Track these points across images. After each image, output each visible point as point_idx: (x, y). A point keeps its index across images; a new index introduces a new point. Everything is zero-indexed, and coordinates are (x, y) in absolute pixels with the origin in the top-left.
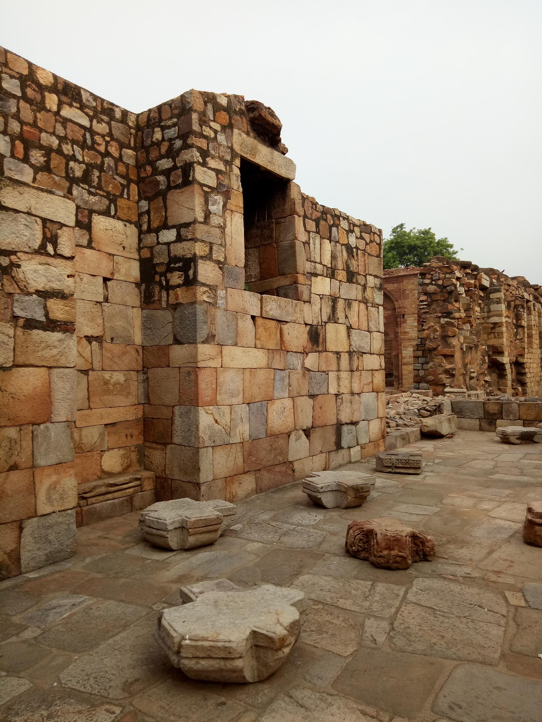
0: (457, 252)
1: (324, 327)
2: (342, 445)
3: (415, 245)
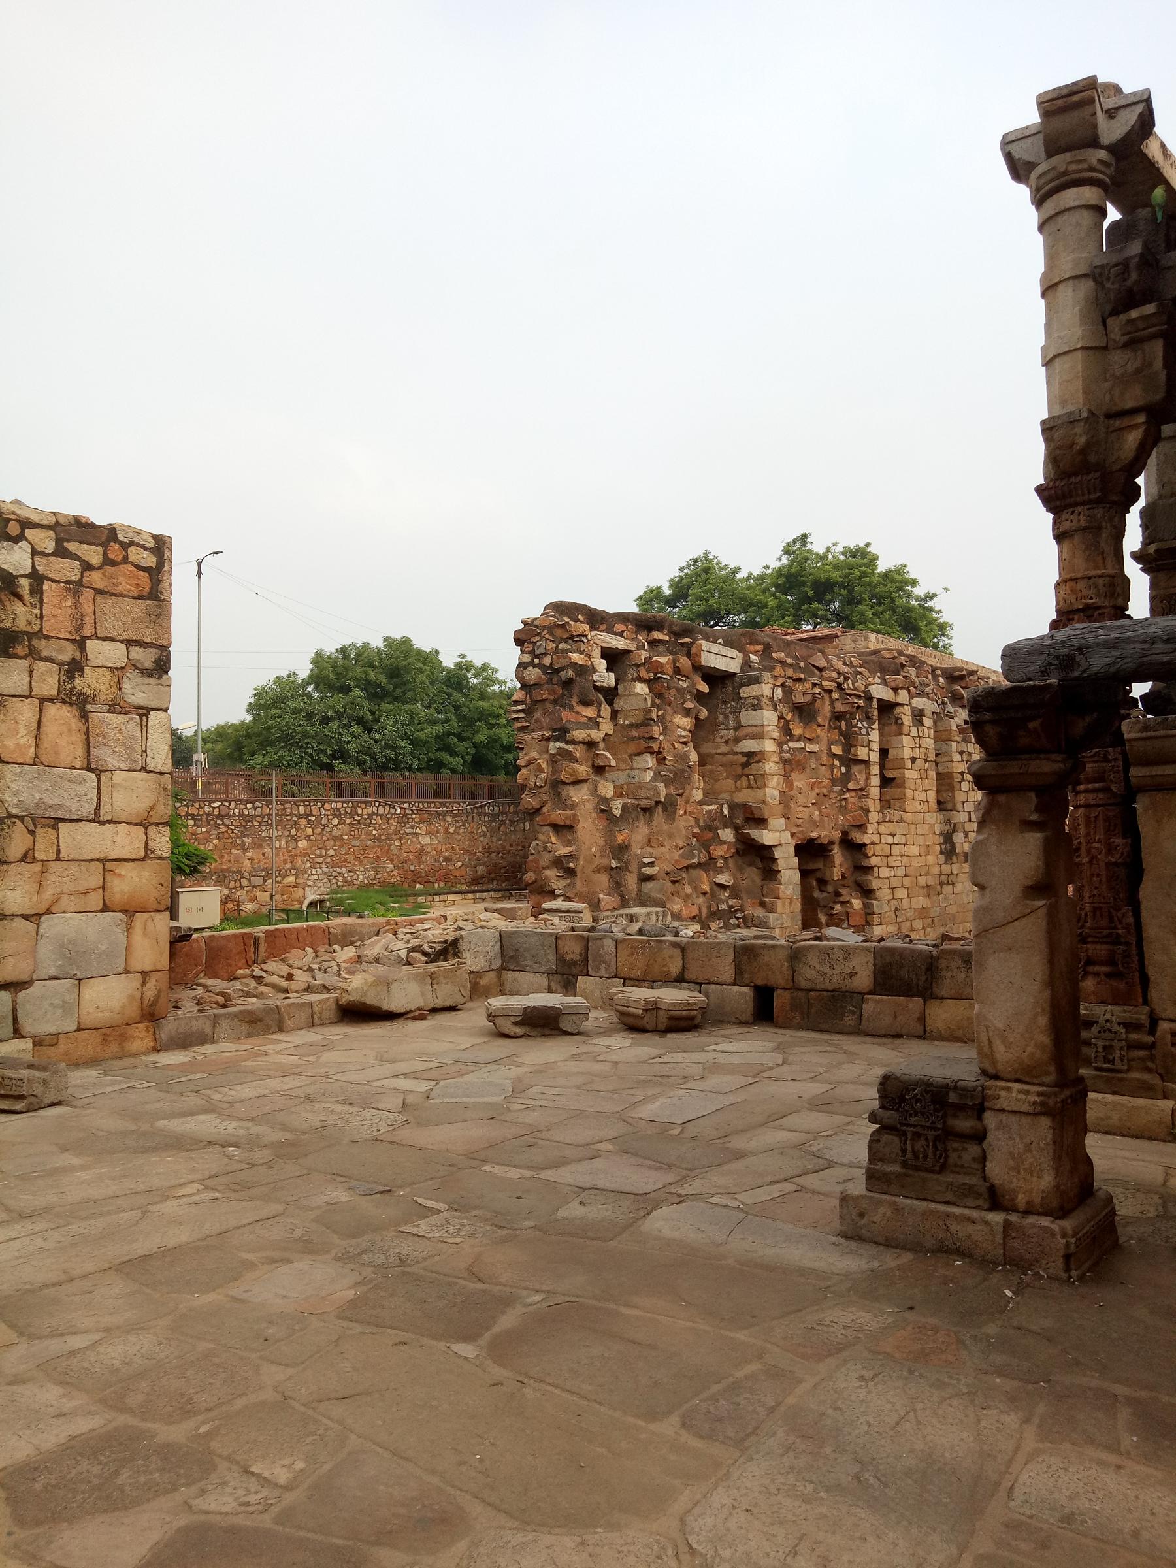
0: (935, 595)
3: (828, 579)
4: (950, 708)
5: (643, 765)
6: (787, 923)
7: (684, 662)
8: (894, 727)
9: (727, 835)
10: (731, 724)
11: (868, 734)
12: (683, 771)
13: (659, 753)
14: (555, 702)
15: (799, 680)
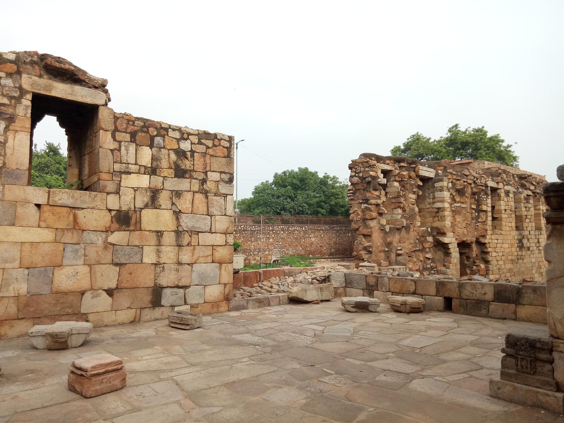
0: (511, 146)
1: (138, 213)
2: (162, 303)
3: (467, 141)
4: (520, 190)
5: (397, 213)
6: (454, 273)
7: (413, 174)
8: (497, 198)
9: (430, 239)
10: (431, 197)
11: (486, 200)
12: (413, 215)
13: (403, 208)
14: (364, 190)
15: (458, 180)
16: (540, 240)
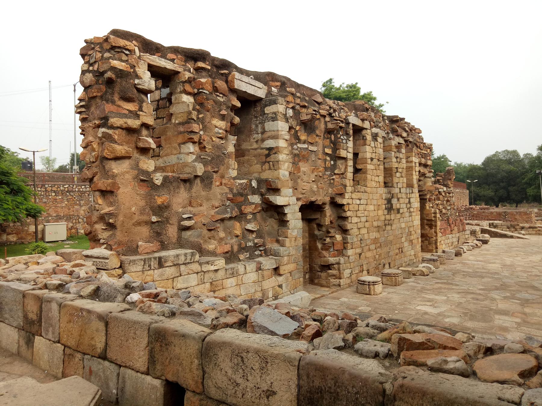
4: (391, 136)
5: (187, 151)
6: (293, 252)
7: (221, 84)
8: (362, 141)
9: (256, 199)
10: (260, 130)
11: (346, 143)
12: (218, 156)
13: (200, 143)
14: (101, 97)
15: (304, 107)
16: (412, 200)
